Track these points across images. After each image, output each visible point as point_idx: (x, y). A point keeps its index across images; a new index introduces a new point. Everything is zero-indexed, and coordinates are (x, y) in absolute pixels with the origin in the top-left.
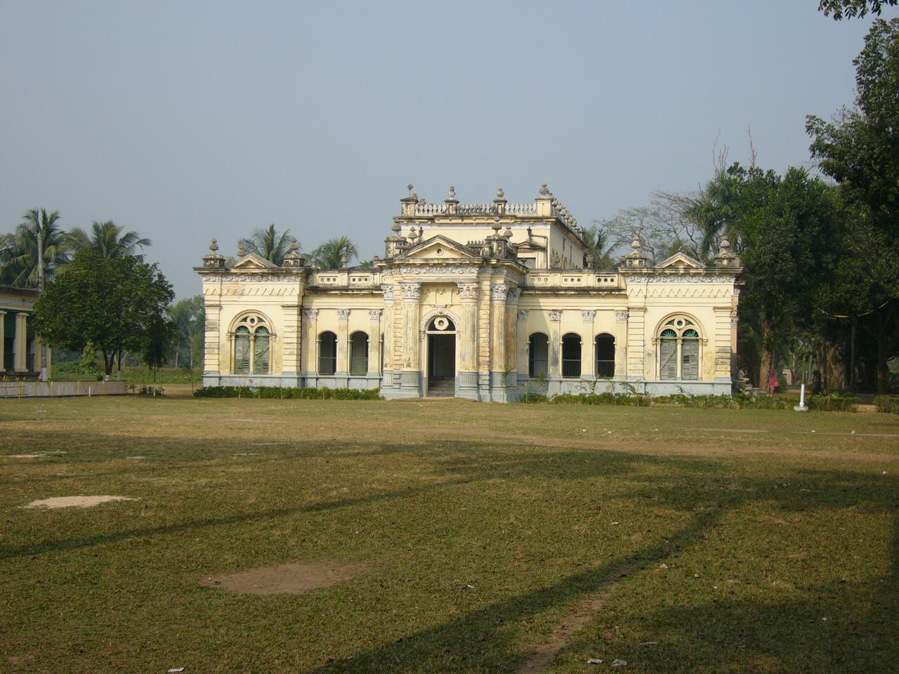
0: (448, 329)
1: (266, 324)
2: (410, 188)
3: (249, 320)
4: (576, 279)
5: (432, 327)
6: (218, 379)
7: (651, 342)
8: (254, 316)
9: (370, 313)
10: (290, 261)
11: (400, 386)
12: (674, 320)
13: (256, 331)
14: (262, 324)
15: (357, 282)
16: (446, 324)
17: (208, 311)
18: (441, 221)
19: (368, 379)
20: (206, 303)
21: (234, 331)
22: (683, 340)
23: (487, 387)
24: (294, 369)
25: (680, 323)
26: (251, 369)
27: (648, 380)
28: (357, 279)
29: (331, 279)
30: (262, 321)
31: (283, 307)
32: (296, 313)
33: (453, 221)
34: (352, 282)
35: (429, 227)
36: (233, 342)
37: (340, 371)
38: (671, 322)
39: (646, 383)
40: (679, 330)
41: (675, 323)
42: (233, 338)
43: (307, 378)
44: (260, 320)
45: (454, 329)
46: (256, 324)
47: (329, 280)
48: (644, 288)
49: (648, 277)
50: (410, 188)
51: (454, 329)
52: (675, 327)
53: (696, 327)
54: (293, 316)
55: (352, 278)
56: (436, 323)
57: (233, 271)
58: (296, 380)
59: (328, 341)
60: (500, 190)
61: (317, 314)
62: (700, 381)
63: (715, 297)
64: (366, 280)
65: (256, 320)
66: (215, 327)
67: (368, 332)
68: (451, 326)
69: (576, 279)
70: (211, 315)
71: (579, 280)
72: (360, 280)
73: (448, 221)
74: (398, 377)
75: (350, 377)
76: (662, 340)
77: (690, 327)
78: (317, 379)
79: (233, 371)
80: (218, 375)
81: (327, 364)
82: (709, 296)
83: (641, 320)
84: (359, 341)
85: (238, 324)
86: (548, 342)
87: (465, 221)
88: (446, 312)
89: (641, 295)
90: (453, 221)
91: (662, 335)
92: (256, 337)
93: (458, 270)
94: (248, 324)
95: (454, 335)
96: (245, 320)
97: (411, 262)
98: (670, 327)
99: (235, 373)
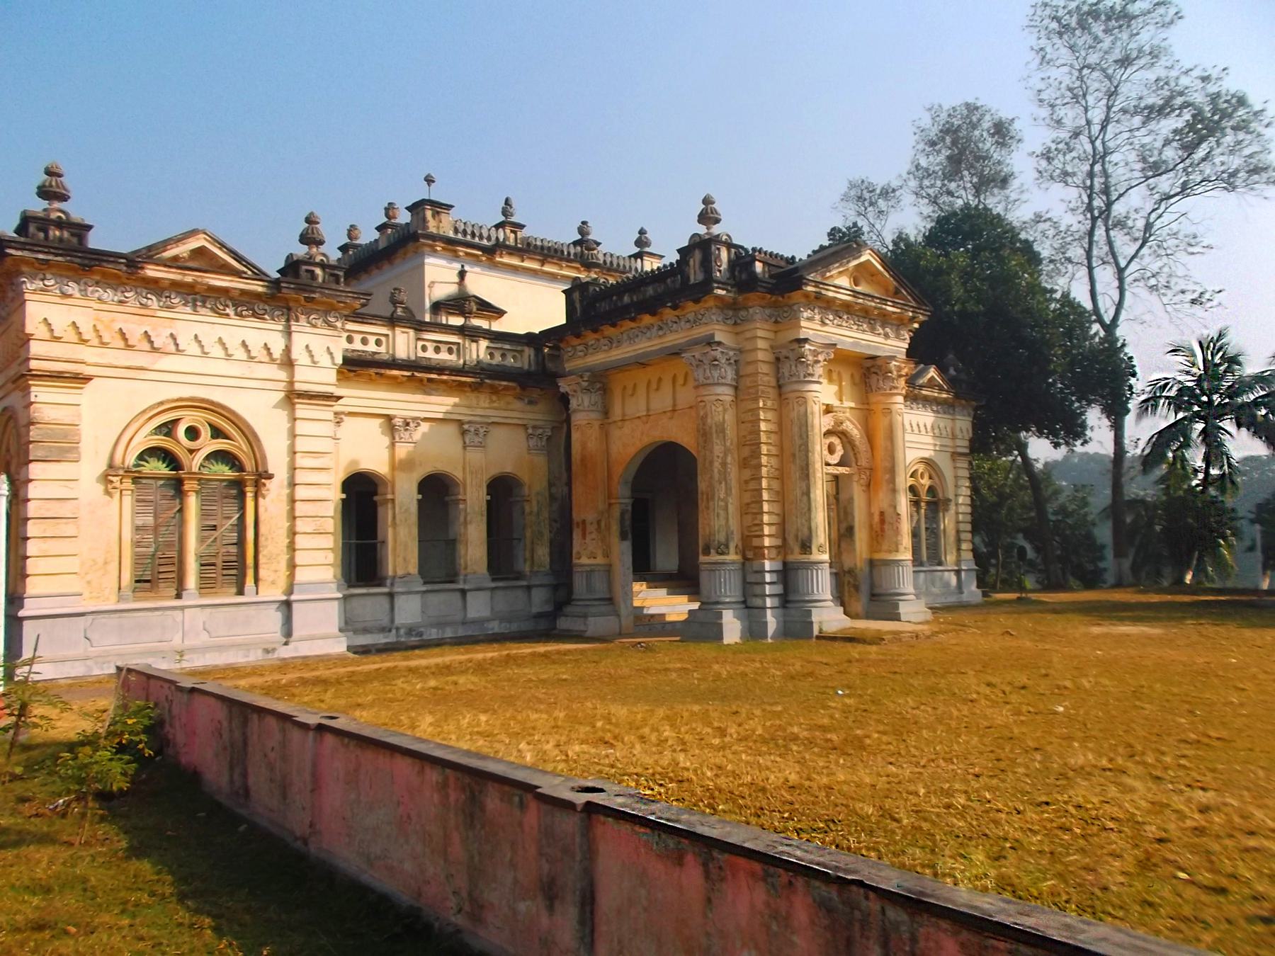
2: (429, 180)
3: (181, 431)
9: (464, 433)
10: (318, 271)
15: (430, 354)
18: (506, 260)
20: (33, 364)
21: (131, 460)
26: (192, 581)
28: (430, 346)
29: (372, 339)
33: (527, 264)
34: (421, 354)
35: (477, 269)
36: (128, 500)
37: (400, 572)
42: (128, 484)
46: (208, 444)
47: (364, 341)
50: (429, 180)
55: (420, 344)
57: (151, 272)
60: (584, 223)
64: (450, 351)
65: (206, 433)
66: (66, 449)
67: (458, 474)
70: (47, 402)
73: (515, 261)
79: (127, 592)
87: (547, 268)
90: (527, 264)
96: (168, 429)
97: (831, 294)
99: (136, 599)
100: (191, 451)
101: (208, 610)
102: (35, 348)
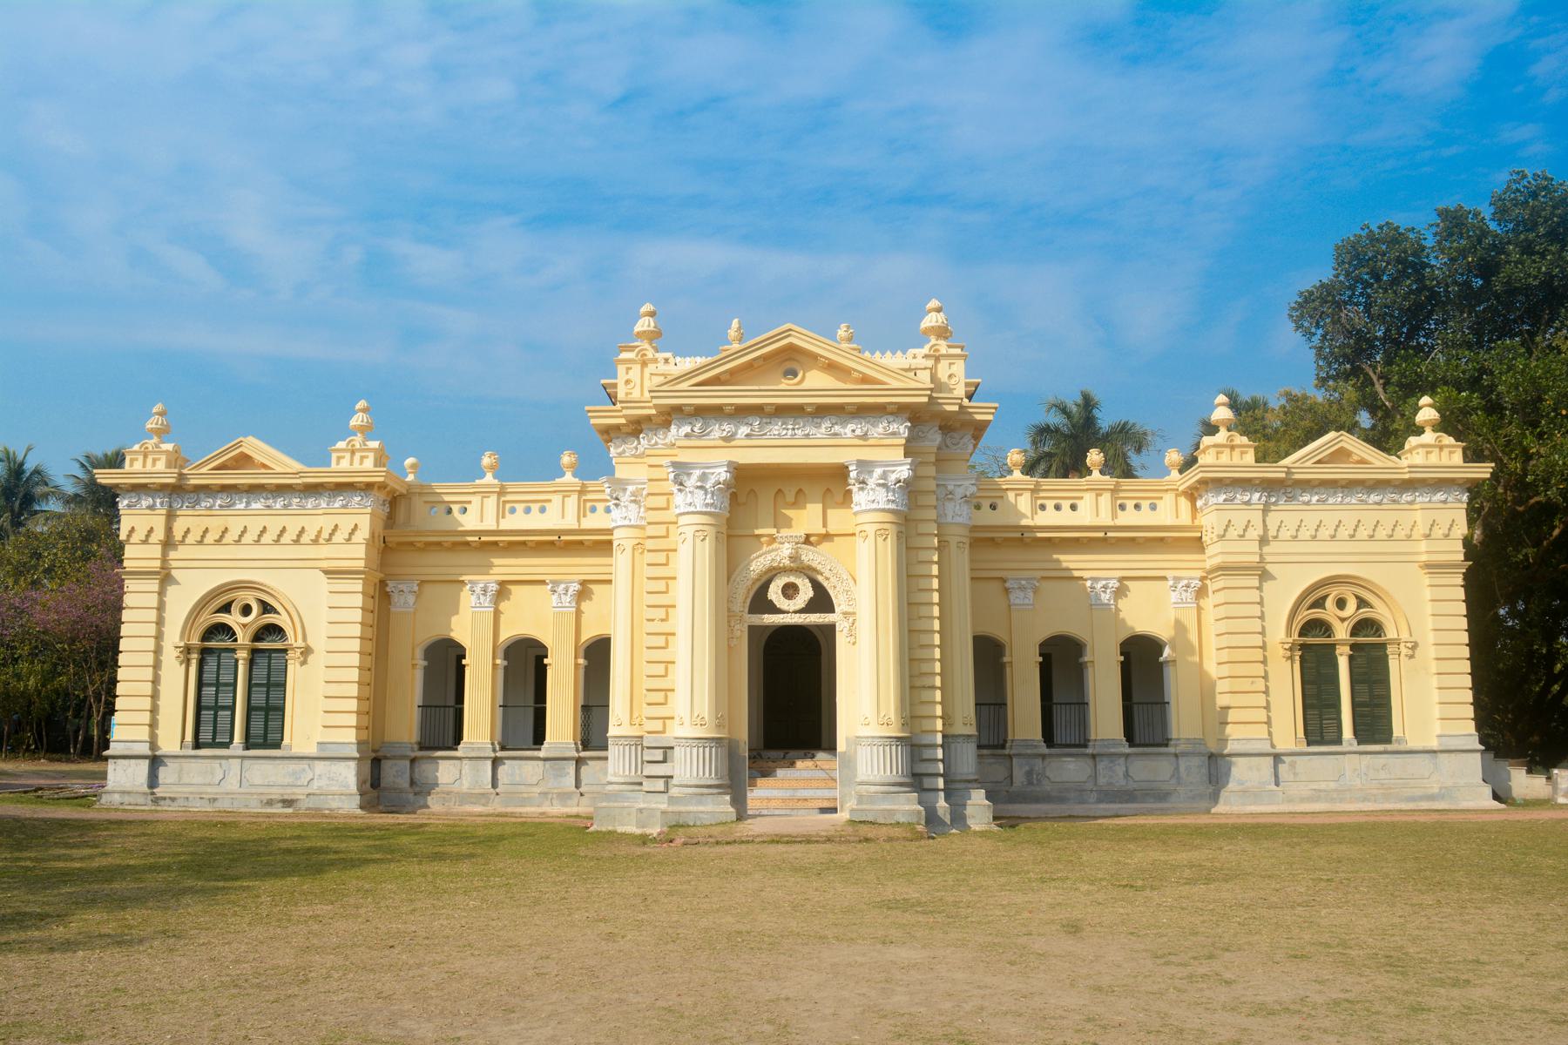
0: (810, 608)
1: (282, 620)
3: (235, 609)
4: (1066, 505)
5: (761, 602)
6: (147, 762)
7: (1282, 652)
8: (250, 598)
11: (667, 784)
12: (1325, 598)
13: (257, 637)
14: (270, 618)
16: (806, 593)
17: (130, 585)
19: (545, 759)
22: (1353, 647)
23: (941, 783)
24: (350, 736)
25: (1341, 604)
27: (1281, 747)
30: (276, 612)
31: (326, 572)
32: (359, 587)
38: (1319, 603)
39: (1277, 758)
40: (1343, 620)
41: (1329, 603)
43: (386, 758)
44: (266, 608)
45: (831, 609)
48: (1256, 517)
49: (1264, 490)
51: (831, 609)
52: (1330, 613)
53: (1380, 612)
54: (352, 599)
56: (774, 593)
58: (353, 764)
59: (446, 662)
61: (418, 595)
62: (1402, 747)
63: (1427, 536)
65: (255, 608)
67: (547, 640)
68: (821, 601)
69: (1066, 505)
71: (1073, 507)
72: (528, 511)
74: (658, 755)
75: (500, 754)
76: (1303, 647)
77: (1365, 613)
78: (413, 761)
80: (144, 749)
81: (443, 728)
82: (1409, 538)
83: (1254, 596)
84: (525, 664)
85: (209, 618)
86: (1006, 659)
88: (809, 556)
89: (1254, 533)
91: (1300, 635)
92: (254, 652)
93: (851, 427)
94: (234, 619)
95: (831, 628)
98: (1317, 613)
100: (244, 626)
101: (246, 762)
102: (129, 552)
